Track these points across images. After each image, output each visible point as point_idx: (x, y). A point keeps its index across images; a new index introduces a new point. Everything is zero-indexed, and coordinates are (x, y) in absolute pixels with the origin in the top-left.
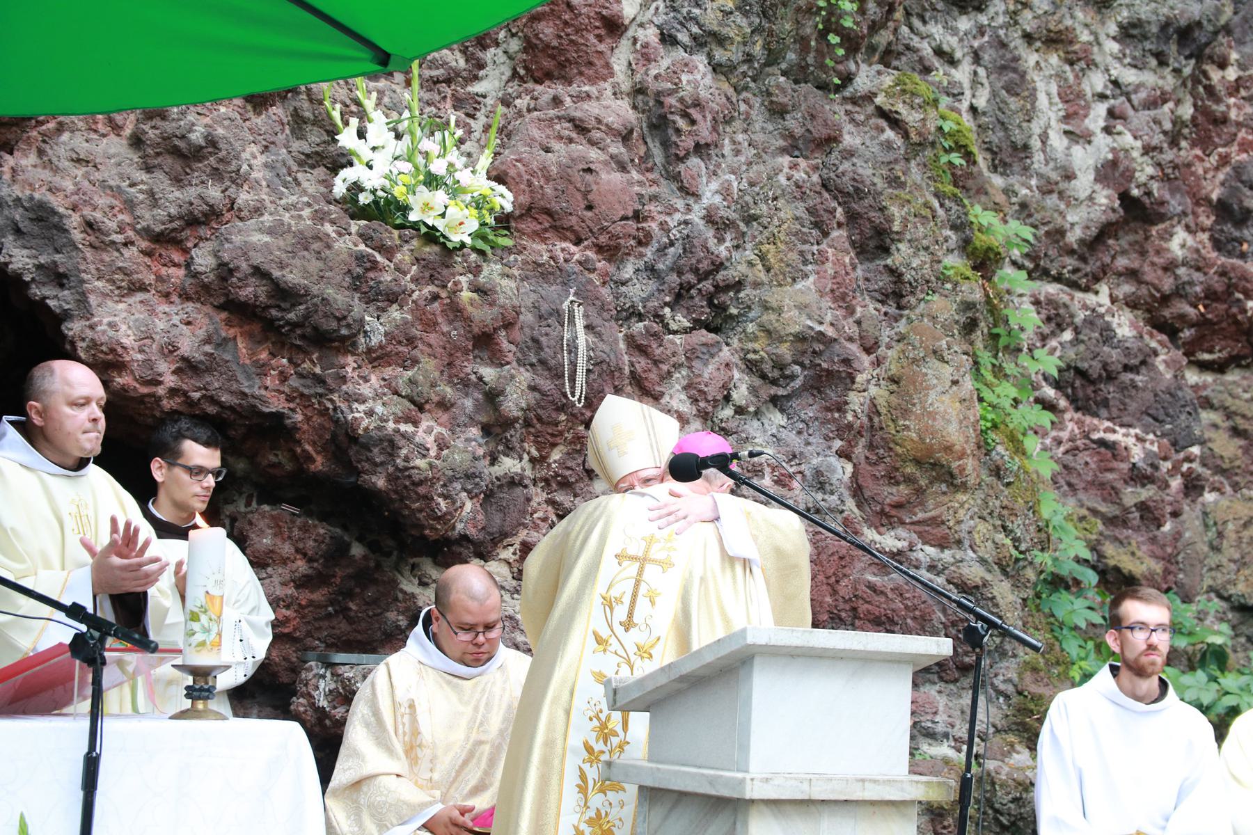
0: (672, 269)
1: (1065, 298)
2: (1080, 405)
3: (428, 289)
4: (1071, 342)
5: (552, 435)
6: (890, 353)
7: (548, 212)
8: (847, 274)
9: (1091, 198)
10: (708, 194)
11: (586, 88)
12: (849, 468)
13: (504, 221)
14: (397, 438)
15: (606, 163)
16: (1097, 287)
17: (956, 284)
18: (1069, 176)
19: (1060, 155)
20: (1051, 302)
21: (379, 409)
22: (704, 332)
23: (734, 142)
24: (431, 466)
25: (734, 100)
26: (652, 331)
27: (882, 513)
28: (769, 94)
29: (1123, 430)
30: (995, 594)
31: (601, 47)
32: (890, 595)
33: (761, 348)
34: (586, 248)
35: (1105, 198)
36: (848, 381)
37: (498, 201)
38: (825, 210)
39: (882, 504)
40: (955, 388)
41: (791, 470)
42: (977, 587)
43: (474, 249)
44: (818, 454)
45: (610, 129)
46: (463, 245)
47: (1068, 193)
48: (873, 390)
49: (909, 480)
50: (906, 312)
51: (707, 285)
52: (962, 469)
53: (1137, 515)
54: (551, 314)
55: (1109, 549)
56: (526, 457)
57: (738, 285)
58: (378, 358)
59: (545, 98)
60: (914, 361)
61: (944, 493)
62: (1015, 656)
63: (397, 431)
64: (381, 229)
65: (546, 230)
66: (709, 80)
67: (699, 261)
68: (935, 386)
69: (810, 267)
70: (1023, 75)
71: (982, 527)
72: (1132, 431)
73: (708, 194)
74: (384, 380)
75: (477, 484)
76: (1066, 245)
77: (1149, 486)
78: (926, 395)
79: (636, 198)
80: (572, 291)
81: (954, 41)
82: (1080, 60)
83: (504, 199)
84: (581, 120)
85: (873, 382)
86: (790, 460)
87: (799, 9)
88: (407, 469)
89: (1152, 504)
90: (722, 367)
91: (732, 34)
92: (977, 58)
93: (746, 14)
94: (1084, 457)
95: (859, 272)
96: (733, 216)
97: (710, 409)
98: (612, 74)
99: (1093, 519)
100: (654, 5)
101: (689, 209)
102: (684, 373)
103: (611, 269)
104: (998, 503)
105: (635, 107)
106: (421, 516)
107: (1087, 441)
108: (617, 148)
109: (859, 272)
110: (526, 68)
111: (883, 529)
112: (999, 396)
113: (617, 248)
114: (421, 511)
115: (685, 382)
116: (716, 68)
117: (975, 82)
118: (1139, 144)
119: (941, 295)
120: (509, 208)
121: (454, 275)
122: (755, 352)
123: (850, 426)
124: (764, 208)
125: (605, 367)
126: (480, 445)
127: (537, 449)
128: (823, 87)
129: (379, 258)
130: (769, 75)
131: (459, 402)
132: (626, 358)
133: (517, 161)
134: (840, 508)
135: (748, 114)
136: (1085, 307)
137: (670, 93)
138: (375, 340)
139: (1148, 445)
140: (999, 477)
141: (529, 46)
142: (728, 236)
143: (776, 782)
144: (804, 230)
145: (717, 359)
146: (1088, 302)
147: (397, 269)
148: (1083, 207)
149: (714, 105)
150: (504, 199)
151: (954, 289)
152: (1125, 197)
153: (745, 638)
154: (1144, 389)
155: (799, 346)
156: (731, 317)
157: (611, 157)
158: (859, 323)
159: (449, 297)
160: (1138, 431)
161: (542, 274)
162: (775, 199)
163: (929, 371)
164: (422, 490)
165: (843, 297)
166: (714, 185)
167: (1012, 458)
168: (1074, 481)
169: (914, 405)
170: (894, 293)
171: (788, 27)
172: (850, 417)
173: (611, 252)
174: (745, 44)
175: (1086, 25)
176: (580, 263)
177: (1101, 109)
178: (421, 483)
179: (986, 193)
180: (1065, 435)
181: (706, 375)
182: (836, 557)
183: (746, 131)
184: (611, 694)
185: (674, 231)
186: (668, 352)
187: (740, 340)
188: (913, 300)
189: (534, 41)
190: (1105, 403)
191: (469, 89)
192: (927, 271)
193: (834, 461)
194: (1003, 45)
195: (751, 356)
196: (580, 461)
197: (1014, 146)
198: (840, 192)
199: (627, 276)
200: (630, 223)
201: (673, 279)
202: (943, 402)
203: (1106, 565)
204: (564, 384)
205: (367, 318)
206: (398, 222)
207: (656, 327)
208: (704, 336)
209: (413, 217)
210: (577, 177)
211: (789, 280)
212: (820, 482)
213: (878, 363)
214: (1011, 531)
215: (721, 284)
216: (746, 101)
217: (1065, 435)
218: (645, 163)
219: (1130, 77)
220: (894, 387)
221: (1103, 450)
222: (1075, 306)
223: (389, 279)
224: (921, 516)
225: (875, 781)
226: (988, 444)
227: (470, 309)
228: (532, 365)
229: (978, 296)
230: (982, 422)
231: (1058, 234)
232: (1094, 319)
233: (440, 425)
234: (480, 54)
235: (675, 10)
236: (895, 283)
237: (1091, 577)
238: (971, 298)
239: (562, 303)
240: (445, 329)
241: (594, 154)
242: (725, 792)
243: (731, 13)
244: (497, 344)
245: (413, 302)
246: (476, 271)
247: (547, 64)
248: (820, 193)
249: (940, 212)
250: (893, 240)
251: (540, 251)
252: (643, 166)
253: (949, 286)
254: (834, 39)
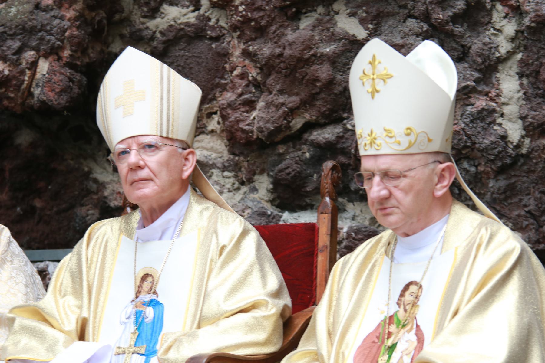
75: (42, 39)
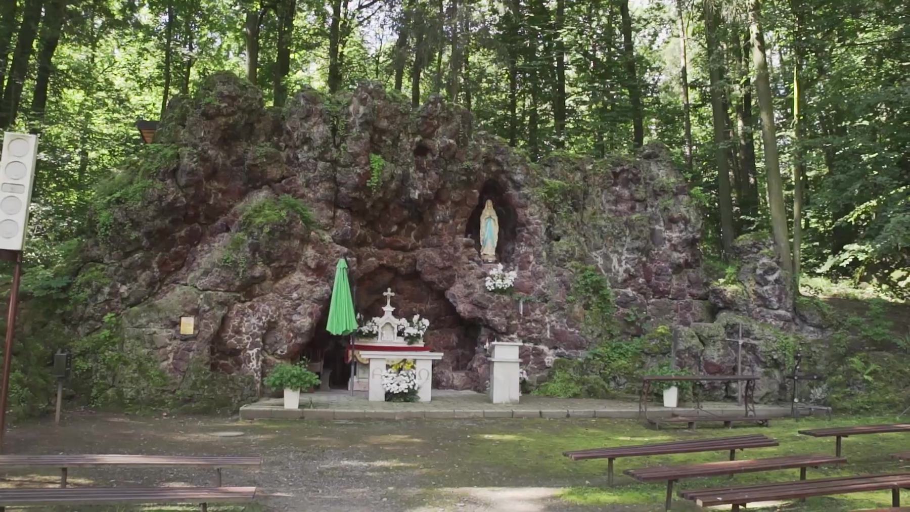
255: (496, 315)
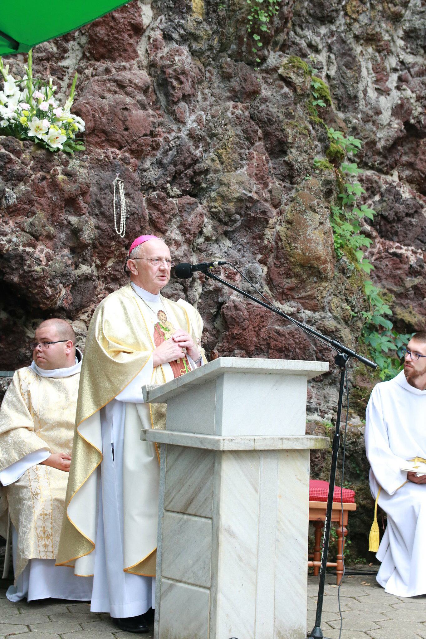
0: (171, 163)
1: (376, 178)
2: (383, 234)
3: (40, 174)
4: (379, 201)
5: (108, 253)
6: (287, 208)
7: (104, 132)
8: (264, 165)
9: (389, 124)
10: (190, 122)
11: (123, 64)
12: (266, 269)
13: (80, 136)
14: (25, 255)
15: (135, 105)
16: (392, 171)
17: (321, 171)
18: (378, 113)
19: (373, 102)
20: (369, 180)
21: (14, 239)
22: (189, 197)
23: (203, 94)
24: (43, 270)
25: (203, 70)
26: (161, 196)
27: (283, 293)
28: (222, 68)
29: (406, 248)
30: (342, 335)
31: (131, 41)
32: (287, 336)
33: (218, 206)
34: (125, 151)
35: (396, 124)
36: (265, 223)
37: (77, 126)
38: (252, 131)
39: (283, 288)
40: (321, 226)
41: (235, 271)
42: (332, 332)
43: (64, 152)
44: (249, 262)
45: (137, 87)
46: (58, 150)
47: (378, 122)
48: (278, 228)
49: (297, 275)
50: (295, 186)
51: (190, 172)
52: (325, 270)
53: (412, 292)
54: (106, 188)
55: (398, 310)
56: (94, 264)
57: (206, 172)
58: (13, 211)
59: (101, 69)
60: (300, 212)
61: (316, 282)
62: (352, 367)
63: (25, 251)
64: (14, 141)
65: (103, 142)
66: (189, 60)
67: (185, 159)
68: (311, 225)
69: (244, 162)
70: (354, 58)
71: (335, 300)
72: (410, 248)
73: (190, 122)
74: (17, 223)
75: (68, 280)
76: (376, 149)
77: (418, 277)
78: (306, 230)
79: (151, 124)
80: (118, 175)
81: (318, 39)
82: (384, 50)
83: (80, 124)
84: (121, 81)
85: (278, 223)
86: (235, 265)
87: (237, 21)
88: (30, 272)
89: (420, 286)
90: (198, 216)
91: (202, 34)
92: (330, 49)
93: (209, 23)
94: (386, 262)
95: (270, 164)
96: (204, 134)
97: (192, 238)
98: (137, 56)
99: (390, 295)
100: (159, 18)
101: (179, 130)
102: (178, 219)
103: (138, 163)
104: (343, 287)
105: (150, 74)
106: (38, 297)
107: (387, 254)
108: (140, 97)
109: (270, 164)
110: (90, 52)
111: (283, 302)
112: (343, 230)
113: (142, 151)
114: (38, 294)
115: (178, 224)
116: (193, 53)
117: (329, 62)
118: (414, 95)
119: (314, 176)
120: (83, 129)
121: (54, 166)
122: (216, 207)
123: (266, 247)
124: (220, 129)
125: (136, 216)
126: (69, 258)
127: (100, 261)
128: (251, 64)
129: (12, 156)
130: (221, 57)
131: (58, 235)
132: (147, 211)
133: (86, 103)
134: (261, 290)
135: (210, 78)
136: (386, 182)
137: (169, 66)
138: (11, 202)
139: (418, 255)
140: (344, 273)
141: (92, 40)
142: (201, 145)
143: (236, 441)
144: (241, 141)
145: (195, 211)
146: (388, 180)
147: (23, 163)
148: (386, 129)
149: (192, 73)
150: (80, 124)
151: (320, 173)
152: (407, 124)
153: (219, 364)
154: (416, 226)
155: (239, 204)
156: (203, 189)
157: (138, 101)
158: (270, 192)
159: (51, 178)
160: (413, 248)
161: (101, 165)
162: (225, 125)
163: (308, 217)
164: (38, 283)
165: (262, 178)
166: (193, 117)
167: (351, 263)
168: (380, 274)
169: (300, 235)
170: (289, 175)
171: (232, 30)
172: (266, 242)
173: (138, 153)
174: (209, 40)
175: (387, 31)
176: (121, 159)
177: (394, 77)
178: (38, 279)
179: (335, 122)
180: (375, 250)
181: (190, 220)
182: (259, 317)
183: (209, 88)
184: (146, 394)
185: (172, 142)
186: (170, 208)
187: (207, 201)
188: (299, 180)
189: (95, 37)
190: (396, 234)
191: (59, 64)
192: (306, 164)
193: (257, 265)
194: (344, 42)
195: (213, 210)
196: (123, 267)
197: (349, 97)
198: (260, 121)
199: (147, 167)
200: (148, 137)
201: (172, 168)
202: (315, 234)
203: (397, 318)
204: (114, 225)
205: (7, 190)
206: (23, 137)
207: (163, 194)
208: (188, 199)
209: (30, 134)
210: (119, 113)
211: (233, 169)
212: (250, 277)
213: (281, 213)
214: (350, 302)
215: (197, 171)
216: (209, 71)
217: (375, 250)
218: (156, 105)
219: (410, 59)
220: (289, 226)
221: (395, 258)
222: (381, 182)
223: (18, 168)
224: (303, 294)
225: (288, 439)
226: (338, 256)
227: (63, 184)
228: (96, 215)
229: (333, 177)
230: (335, 244)
231: (372, 144)
232: (391, 189)
233: (48, 247)
234: (65, 45)
235: (171, 20)
236: (289, 170)
237: (389, 325)
238: (329, 178)
239: (112, 181)
240: (49, 195)
241: (128, 100)
242: (209, 447)
243: (201, 23)
244: (78, 204)
245: (32, 180)
246: (66, 164)
247: (102, 50)
248: (249, 122)
249: (313, 132)
250: (288, 147)
251: (100, 153)
252: (155, 107)
253: (317, 172)
254: (256, 37)
255: (36, 237)
